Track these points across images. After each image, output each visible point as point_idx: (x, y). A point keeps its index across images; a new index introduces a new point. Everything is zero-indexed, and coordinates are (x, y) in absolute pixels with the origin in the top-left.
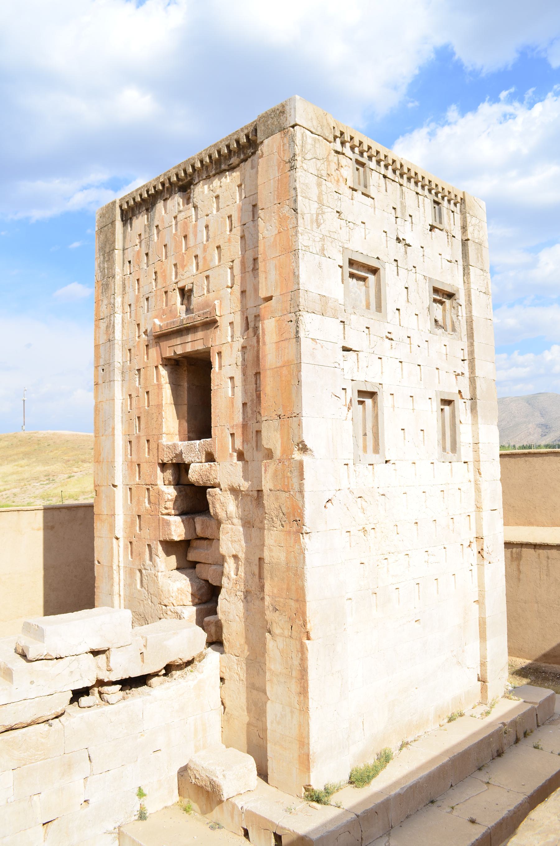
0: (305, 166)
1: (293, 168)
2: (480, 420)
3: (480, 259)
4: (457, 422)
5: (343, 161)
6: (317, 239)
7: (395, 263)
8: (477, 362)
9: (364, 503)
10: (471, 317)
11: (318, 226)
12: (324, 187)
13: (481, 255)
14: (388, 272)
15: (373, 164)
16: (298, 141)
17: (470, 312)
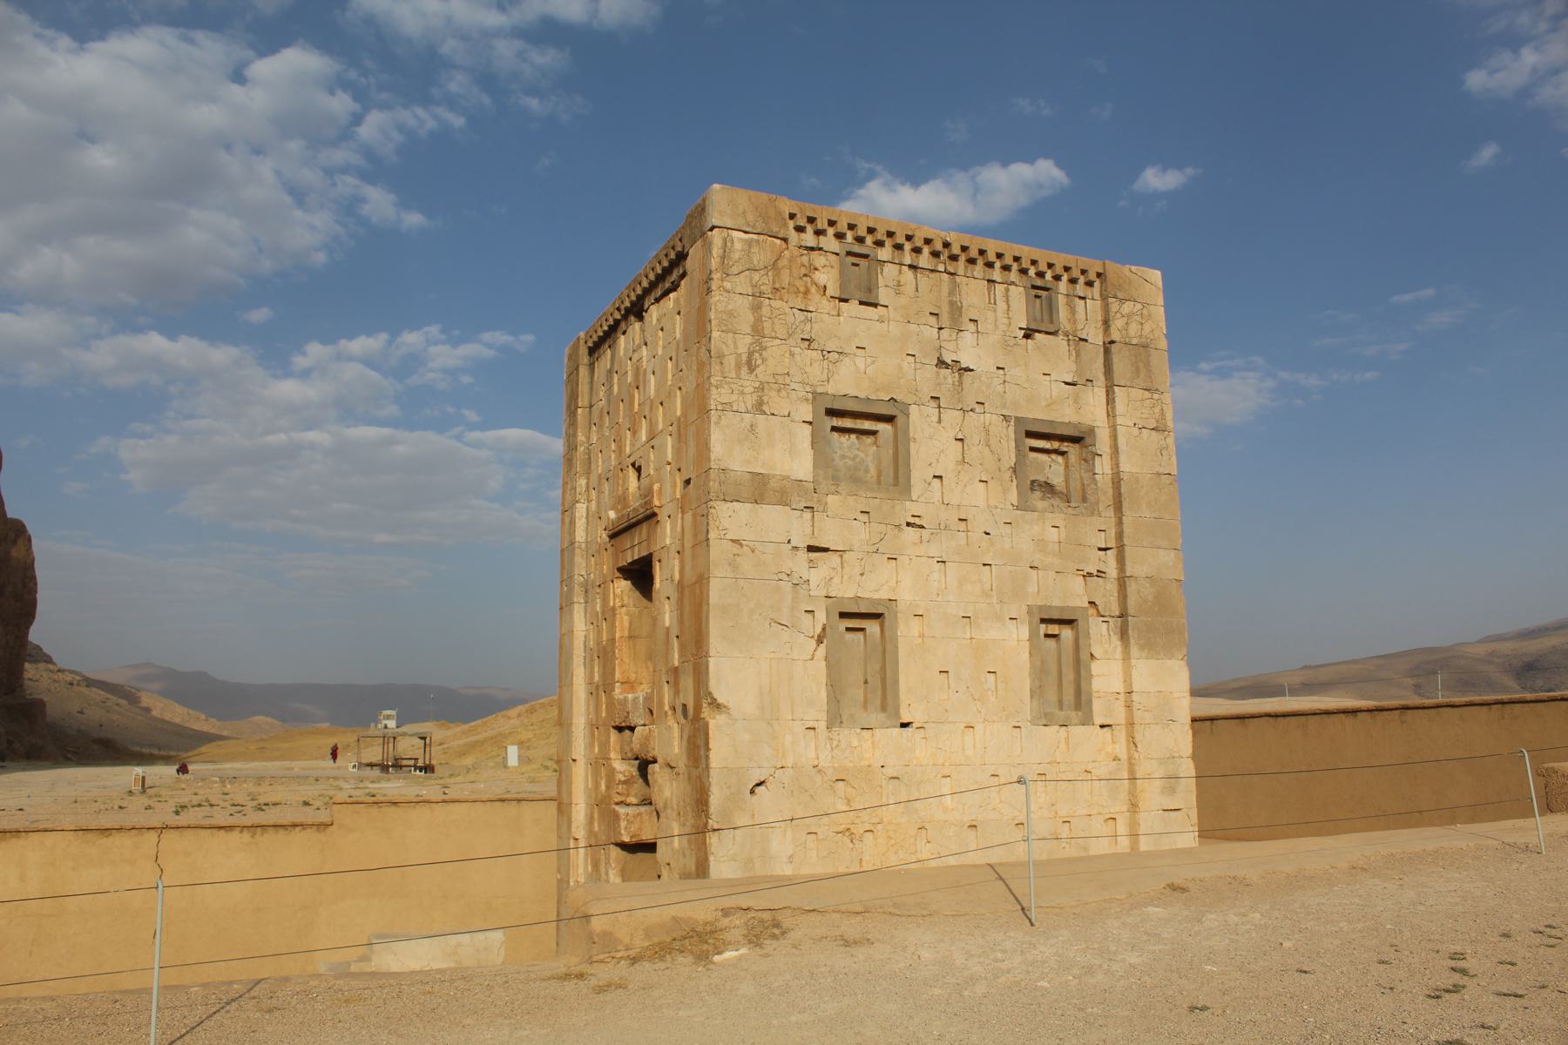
0: (728, 285)
1: (709, 291)
2: (1134, 650)
3: (1143, 373)
4: (1084, 656)
5: (819, 259)
6: (749, 390)
7: (933, 404)
8: (1128, 551)
9: (850, 790)
10: (1118, 473)
11: (752, 368)
12: (765, 311)
13: (1148, 365)
14: (920, 420)
15: (885, 253)
16: (716, 251)
17: (1117, 465)
